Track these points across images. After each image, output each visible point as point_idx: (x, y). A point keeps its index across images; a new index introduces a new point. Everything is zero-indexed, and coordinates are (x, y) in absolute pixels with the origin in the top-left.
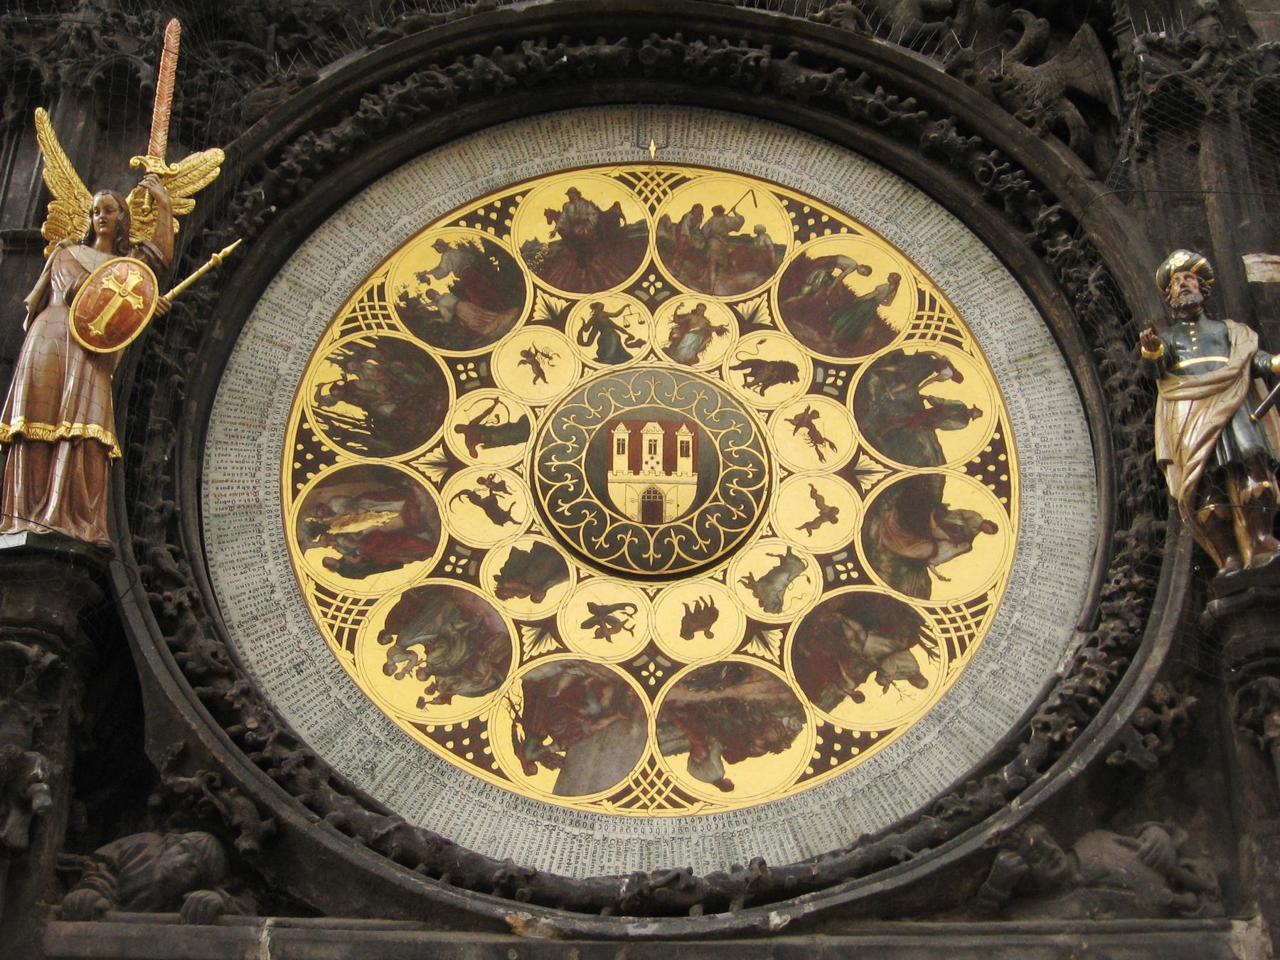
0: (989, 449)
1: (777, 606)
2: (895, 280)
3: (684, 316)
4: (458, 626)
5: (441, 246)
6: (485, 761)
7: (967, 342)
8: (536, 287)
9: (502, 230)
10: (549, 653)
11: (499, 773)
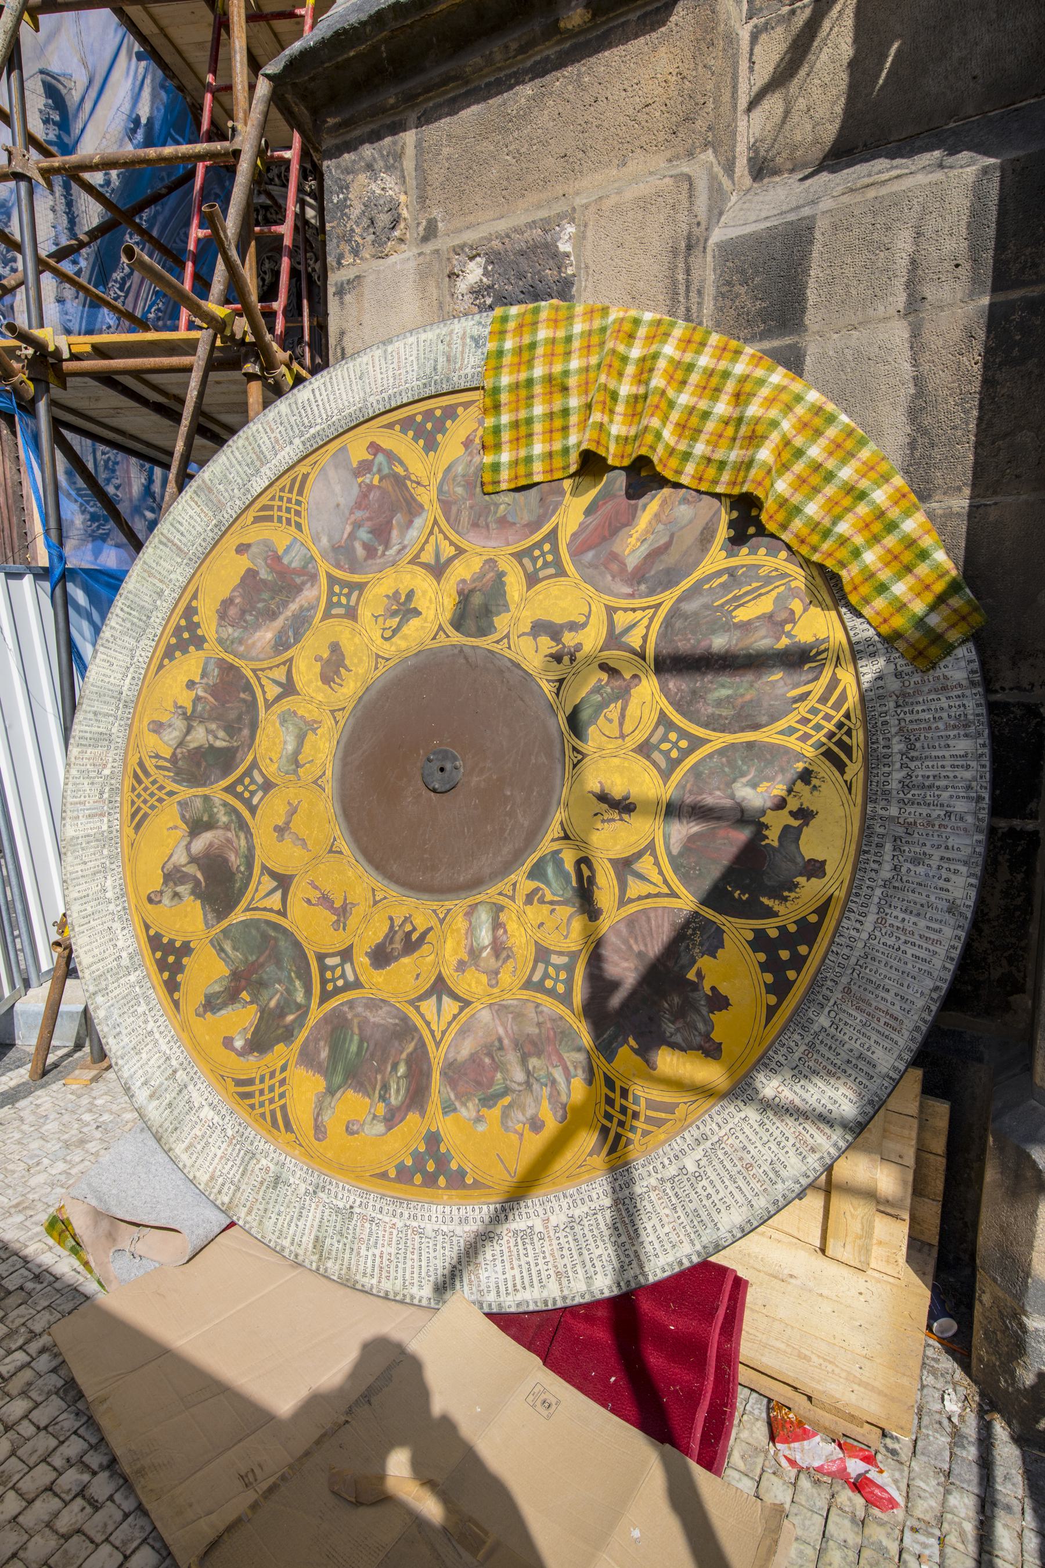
1: (283, 721)
3: (505, 961)
4: (502, 507)
5: (816, 869)
6: (407, 424)
8: (673, 895)
9: (760, 941)
10: (422, 549)
11: (390, 426)
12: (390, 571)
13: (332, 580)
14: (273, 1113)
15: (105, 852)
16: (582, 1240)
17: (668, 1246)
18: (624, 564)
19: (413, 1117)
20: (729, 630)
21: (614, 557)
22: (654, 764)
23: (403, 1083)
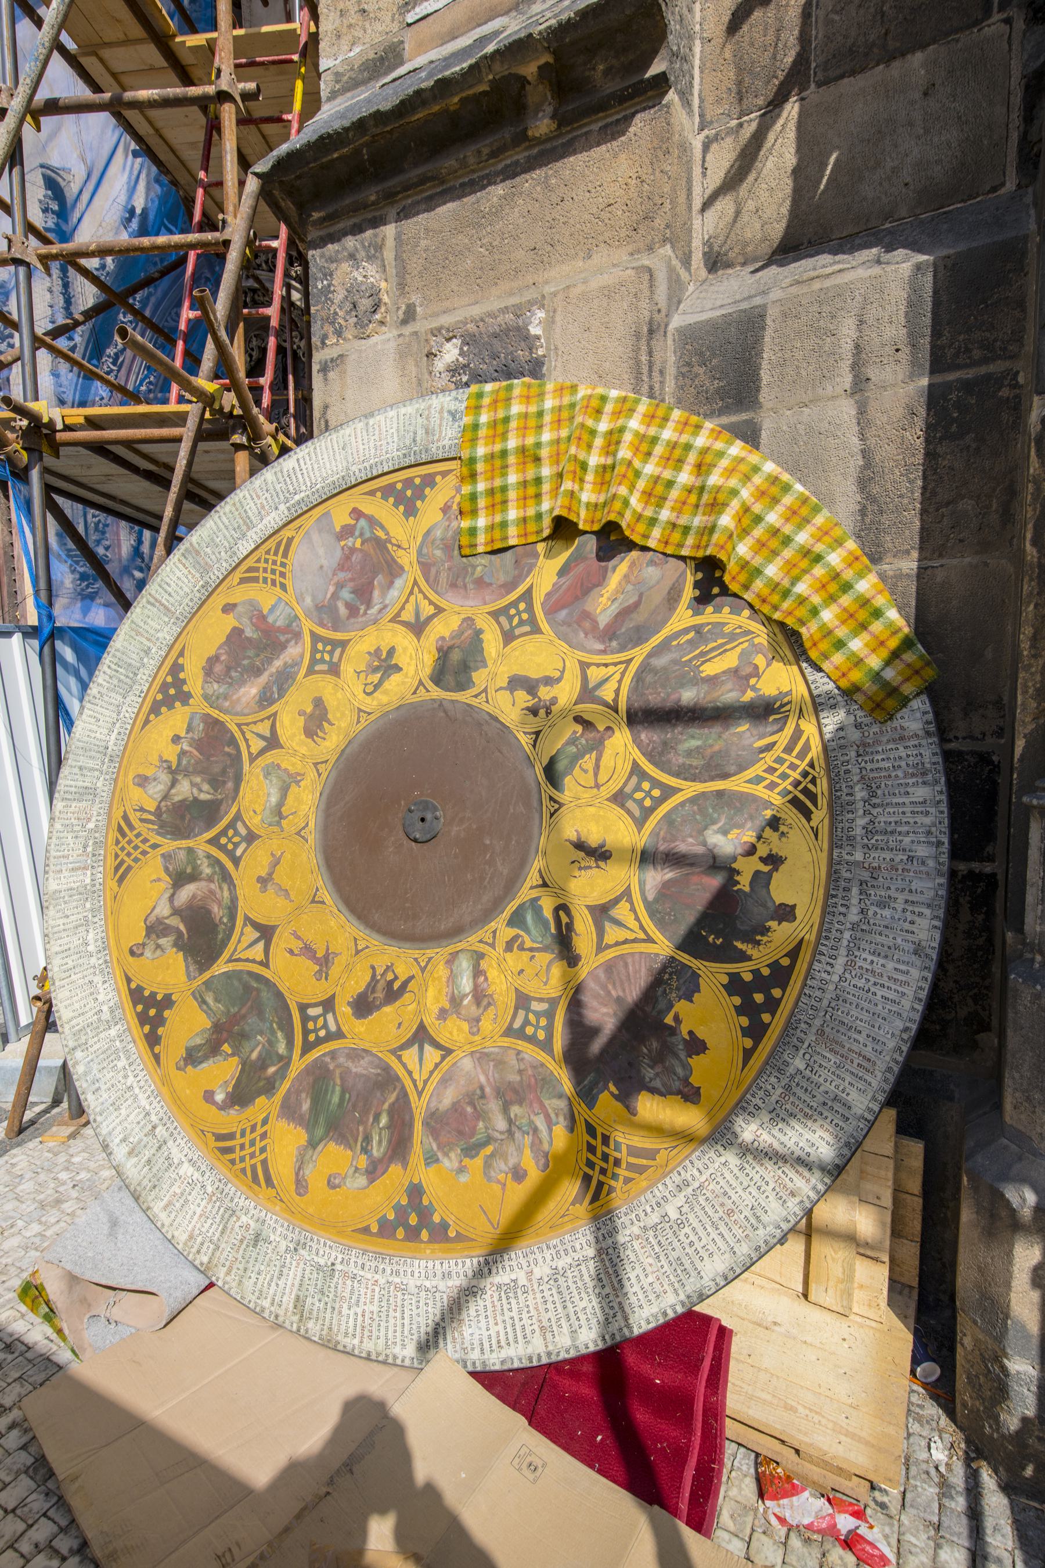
1: (267, 774)
2: (301, 1185)
4: (479, 569)
5: (786, 913)
6: (388, 491)
8: (650, 940)
9: (735, 985)
10: (403, 608)
11: (372, 493)
12: (371, 629)
13: (315, 638)
14: (254, 1168)
15: (88, 905)
16: (566, 1293)
17: (652, 1297)
18: (595, 622)
19: (395, 1169)
20: (696, 684)
21: (586, 615)
22: (629, 812)
23: (385, 1134)
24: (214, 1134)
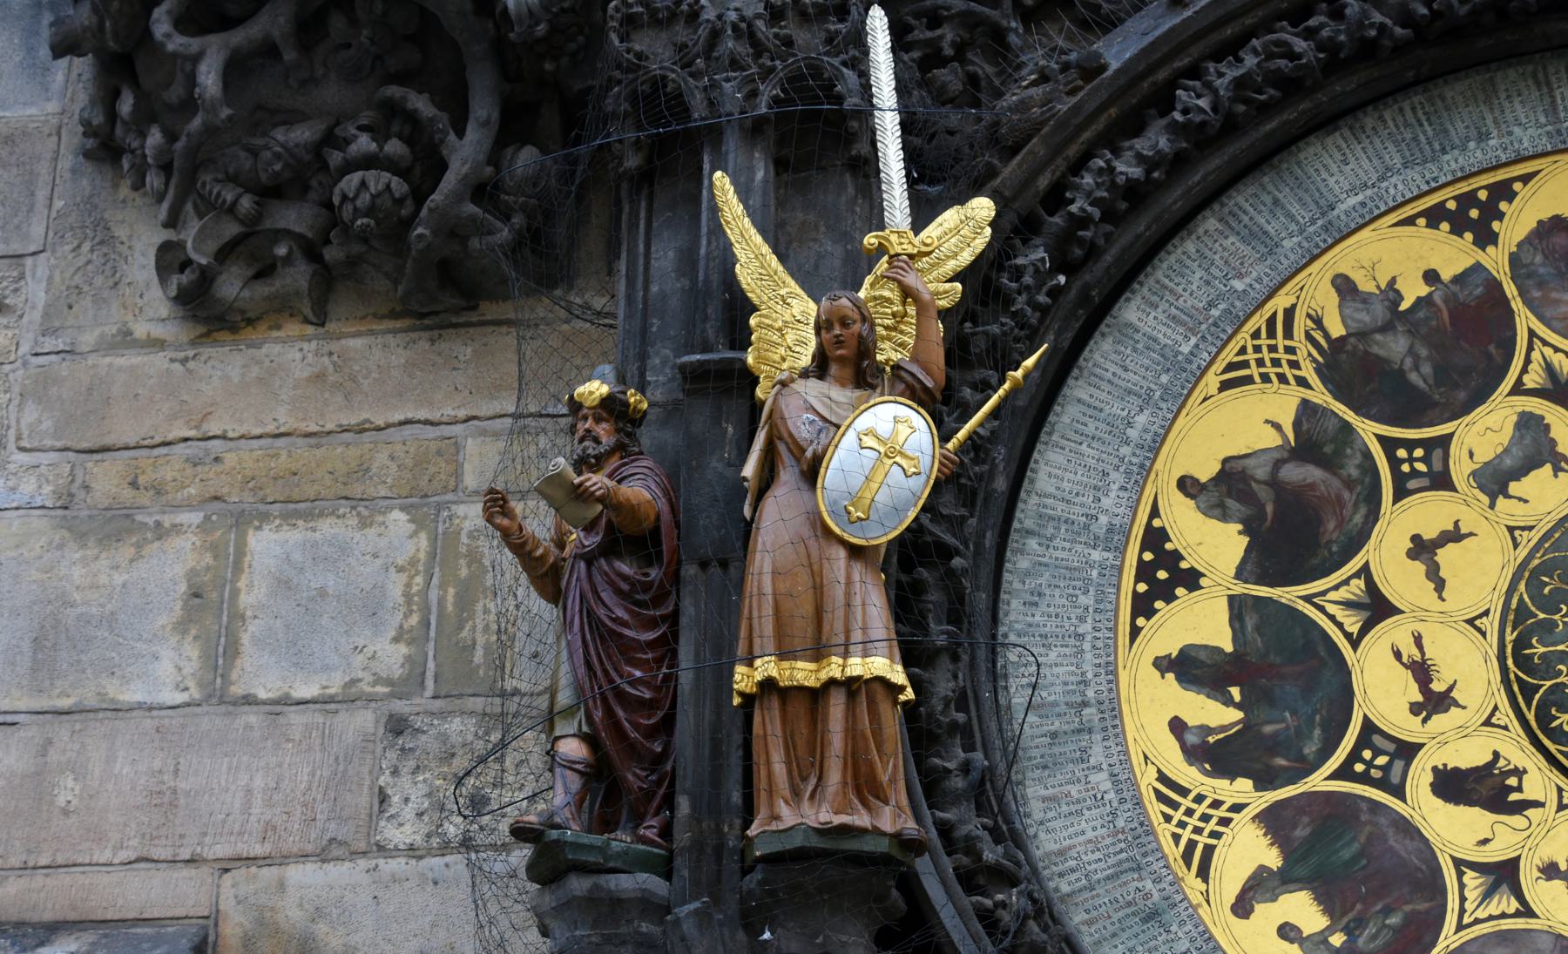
0: (1158, 604)
2: (1242, 908)
7: (1147, 779)
14: (1192, 845)
15: (1164, 379)
24: (1159, 771)
